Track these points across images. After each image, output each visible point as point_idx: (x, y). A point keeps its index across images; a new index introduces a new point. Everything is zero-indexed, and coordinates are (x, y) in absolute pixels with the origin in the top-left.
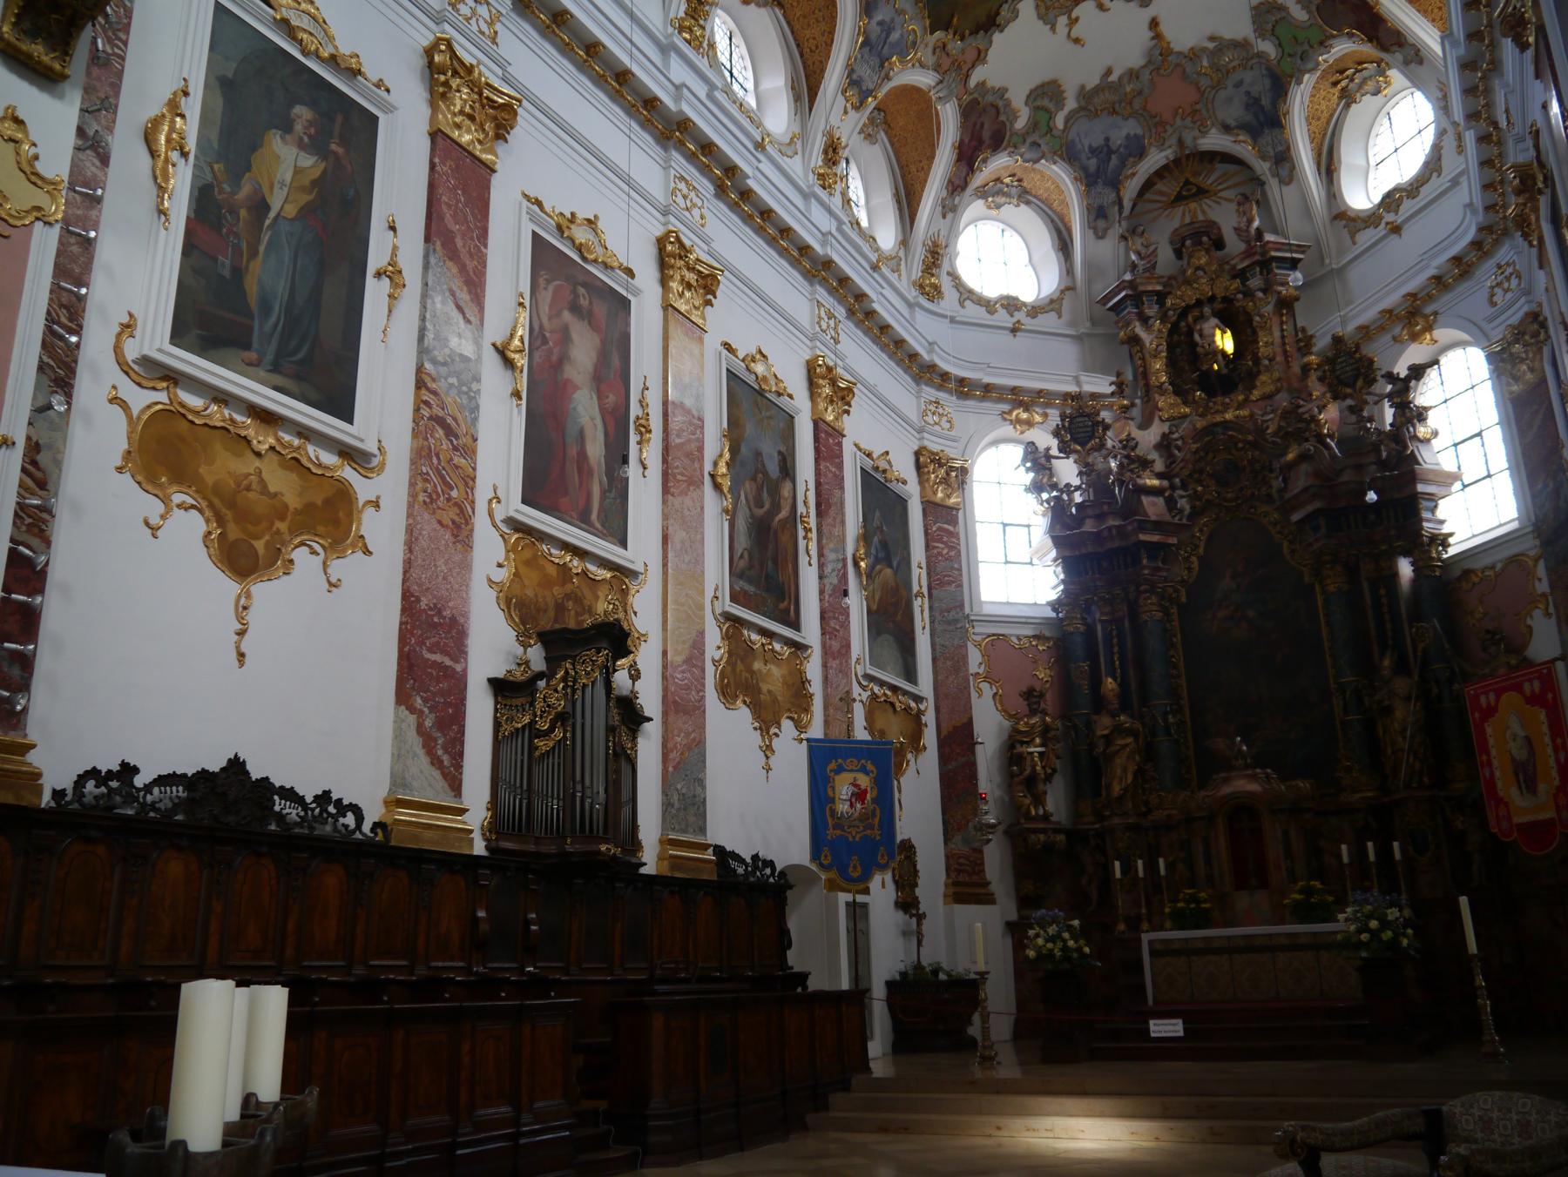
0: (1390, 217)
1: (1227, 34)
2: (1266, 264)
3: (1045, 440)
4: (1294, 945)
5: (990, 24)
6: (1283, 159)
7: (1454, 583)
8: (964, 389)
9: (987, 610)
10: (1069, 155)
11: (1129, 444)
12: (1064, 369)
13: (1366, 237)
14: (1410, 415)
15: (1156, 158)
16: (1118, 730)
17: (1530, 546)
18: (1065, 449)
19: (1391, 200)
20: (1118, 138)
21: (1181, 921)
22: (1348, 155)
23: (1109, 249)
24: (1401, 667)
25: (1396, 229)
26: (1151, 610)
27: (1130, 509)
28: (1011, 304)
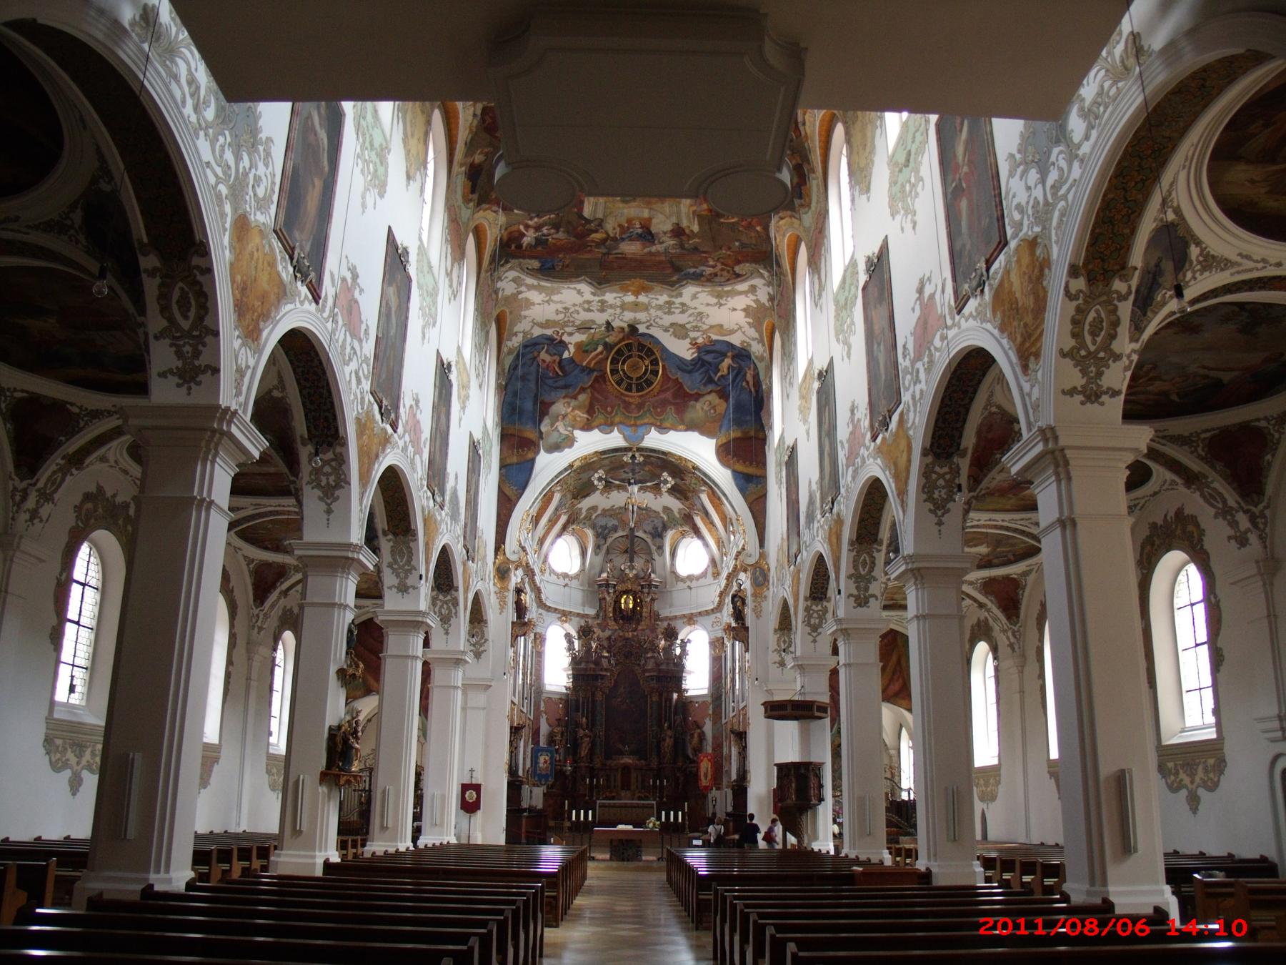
0: (688, 583)
1: (654, 508)
2: (650, 586)
3: (574, 633)
4: (638, 806)
5: (588, 495)
6: (660, 548)
7: (686, 704)
8: (548, 609)
9: (548, 688)
10: (593, 527)
11: (599, 639)
12: (574, 600)
13: (681, 585)
14: (684, 652)
15: (620, 533)
16: (586, 736)
17: (709, 700)
18: (579, 638)
19: (690, 578)
20: (610, 524)
21: (607, 798)
22: (680, 552)
23: (599, 559)
24: (669, 727)
25: (690, 588)
26: (599, 696)
27: (597, 663)
28: (565, 576)
